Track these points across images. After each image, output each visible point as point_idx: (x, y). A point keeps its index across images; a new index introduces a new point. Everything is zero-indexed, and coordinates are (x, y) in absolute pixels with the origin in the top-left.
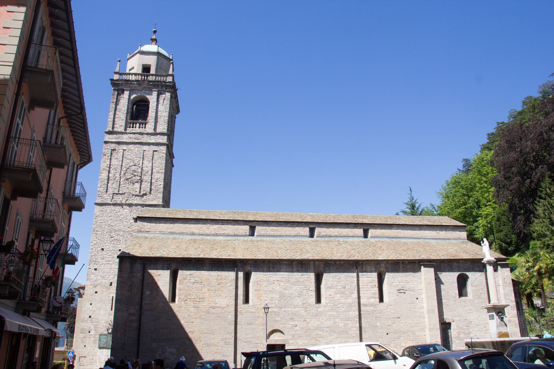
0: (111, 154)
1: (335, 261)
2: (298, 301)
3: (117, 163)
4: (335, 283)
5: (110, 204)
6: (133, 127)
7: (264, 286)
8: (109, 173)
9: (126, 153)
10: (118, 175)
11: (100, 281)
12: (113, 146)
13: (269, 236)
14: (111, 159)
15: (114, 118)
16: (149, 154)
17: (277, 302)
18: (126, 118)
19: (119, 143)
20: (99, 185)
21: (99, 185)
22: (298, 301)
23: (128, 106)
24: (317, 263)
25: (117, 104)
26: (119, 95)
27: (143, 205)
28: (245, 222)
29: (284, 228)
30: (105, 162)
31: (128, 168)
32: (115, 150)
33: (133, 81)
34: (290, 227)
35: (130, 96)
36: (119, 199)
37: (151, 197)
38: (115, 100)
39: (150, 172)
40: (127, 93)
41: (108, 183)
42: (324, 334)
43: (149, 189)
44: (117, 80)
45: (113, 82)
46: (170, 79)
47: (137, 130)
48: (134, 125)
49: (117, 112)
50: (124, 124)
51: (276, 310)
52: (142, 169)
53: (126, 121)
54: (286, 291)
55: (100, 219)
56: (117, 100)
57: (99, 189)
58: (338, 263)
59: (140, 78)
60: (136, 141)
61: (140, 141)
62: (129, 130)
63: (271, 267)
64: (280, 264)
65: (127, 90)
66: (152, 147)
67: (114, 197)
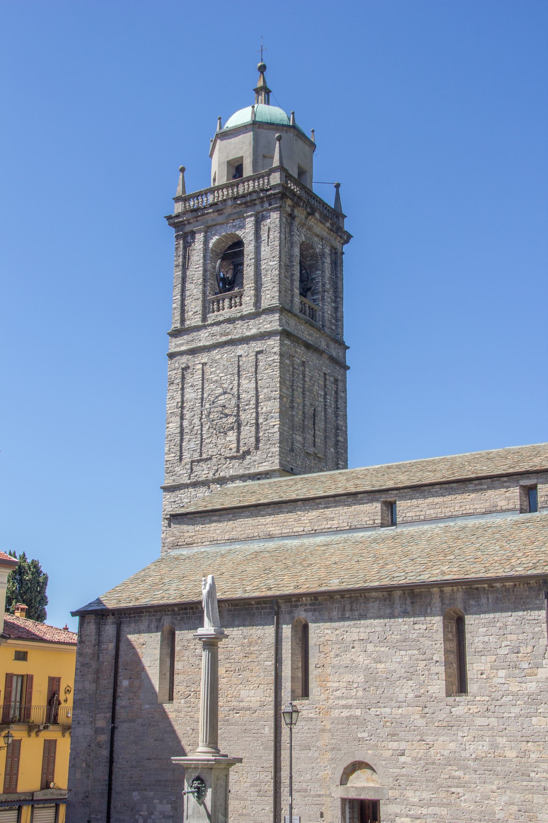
0: (183, 378)
1: (491, 581)
2: (406, 690)
3: (193, 395)
4: (492, 639)
5: (187, 486)
6: (219, 310)
7: (332, 654)
8: (182, 418)
9: (207, 369)
10: (196, 421)
12: (184, 359)
13: (425, 521)
14: (183, 389)
15: (183, 300)
16: (248, 363)
17: (360, 693)
18: (204, 293)
19: (193, 352)
21: (167, 449)
22: (406, 690)
23: (205, 264)
24: (447, 589)
25: (185, 267)
26: (187, 245)
27: (243, 478)
28: (371, 495)
29: (459, 497)
30: (173, 398)
31: (213, 402)
32: (188, 367)
33: (205, 208)
34: (473, 491)
35: (206, 243)
36: (203, 472)
37: (257, 456)
38: (181, 260)
39: (253, 402)
41: (182, 440)
42: (467, 777)
43: (253, 440)
44: (177, 216)
45: (171, 221)
46: (276, 179)
47: (226, 313)
48: (221, 305)
49: (188, 286)
50: (199, 308)
51: (358, 712)
52: (239, 398)
53: (204, 300)
54: (381, 666)
56: (184, 257)
57: (167, 458)
58: (498, 585)
59: (221, 195)
60: (224, 339)
61: (230, 337)
62: (212, 318)
63: (348, 607)
64: (367, 599)
65: (199, 232)
66: (253, 344)
67: (195, 468)
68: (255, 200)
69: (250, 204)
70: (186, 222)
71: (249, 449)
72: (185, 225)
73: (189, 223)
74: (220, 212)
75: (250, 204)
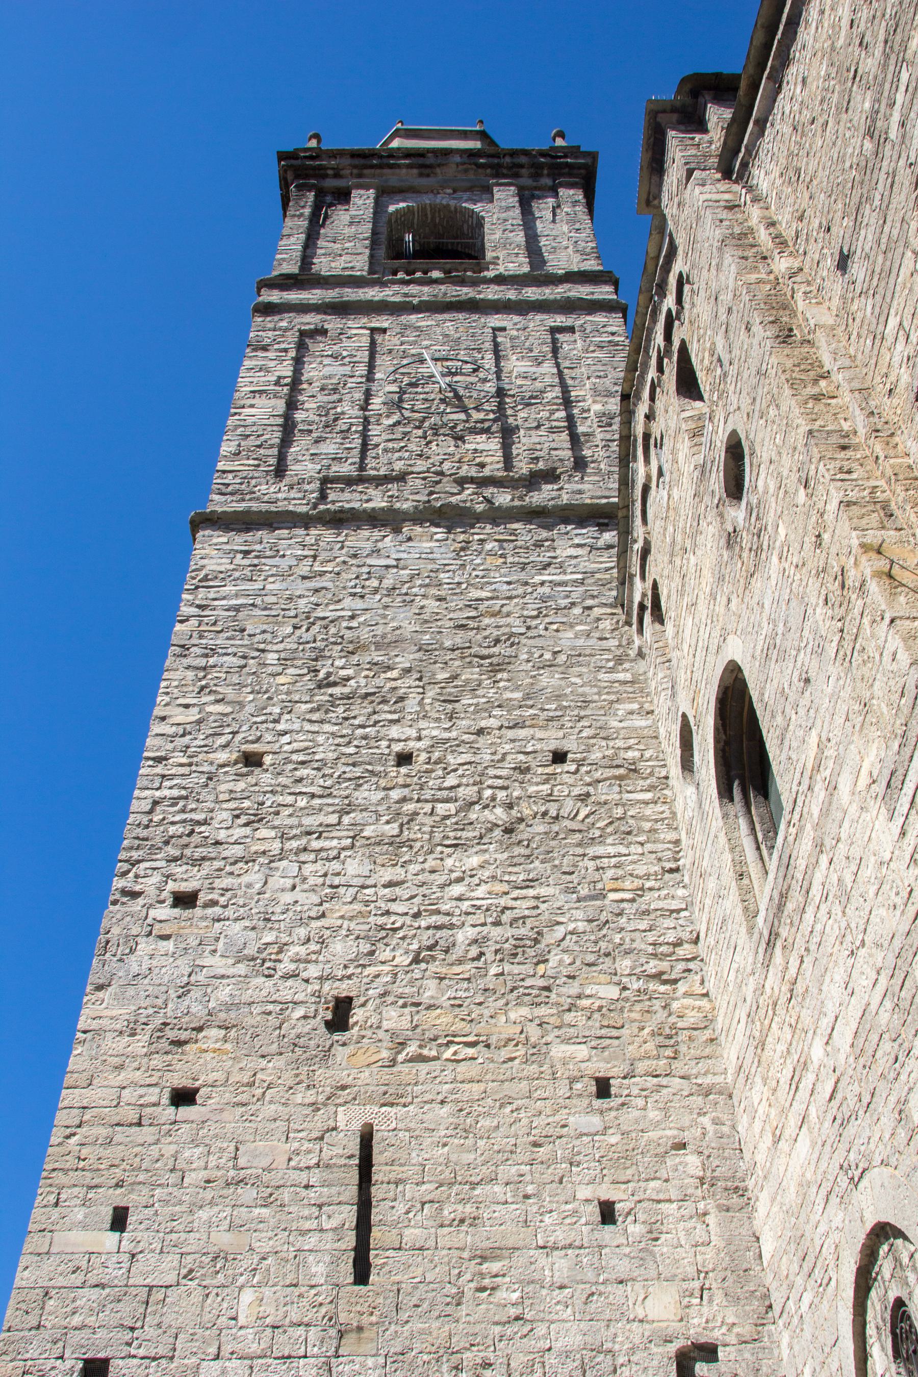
5: (305, 521)
11: (224, 993)
20: (227, 448)
40: (363, 201)
55: (229, 589)
68: (522, 166)
69: (505, 171)
70: (330, 172)
71: (555, 469)
72: (325, 176)
73: (337, 176)
74: (427, 171)
75: (505, 171)
